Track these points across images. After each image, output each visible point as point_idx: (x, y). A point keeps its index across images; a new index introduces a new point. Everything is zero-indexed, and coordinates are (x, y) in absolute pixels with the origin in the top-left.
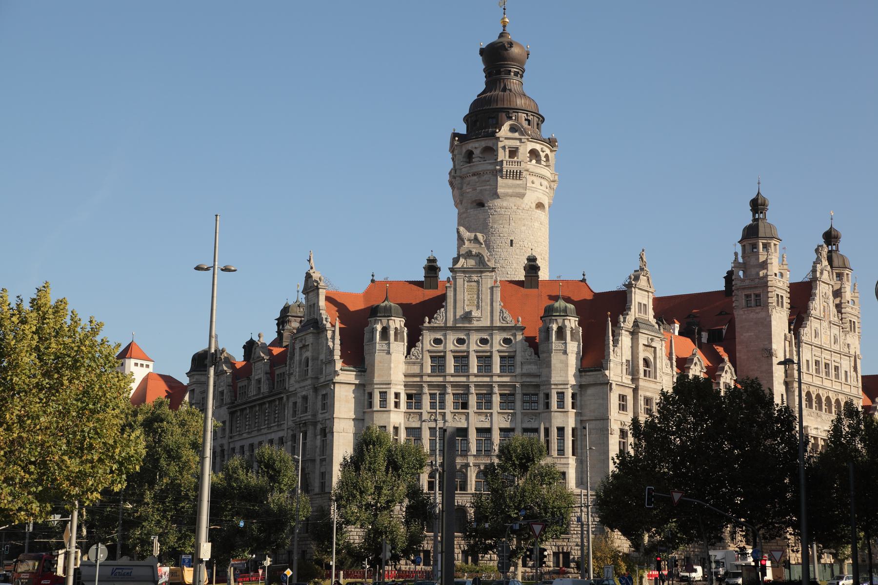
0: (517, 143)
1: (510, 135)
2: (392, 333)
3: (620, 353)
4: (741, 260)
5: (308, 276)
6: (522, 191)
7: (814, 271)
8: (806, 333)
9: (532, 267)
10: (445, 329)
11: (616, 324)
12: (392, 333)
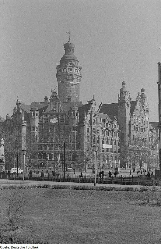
0: (72, 68)
1: (70, 65)
2: (36, 114)
3: (87, 118)
4: (120, 96)
5: (17, 101)
6: (73, 79)
7: (137, 99)
8: (135, 113)
9: (69, 99)
10: (48, 113)
11: (87, 112)
12: (36, 114)
